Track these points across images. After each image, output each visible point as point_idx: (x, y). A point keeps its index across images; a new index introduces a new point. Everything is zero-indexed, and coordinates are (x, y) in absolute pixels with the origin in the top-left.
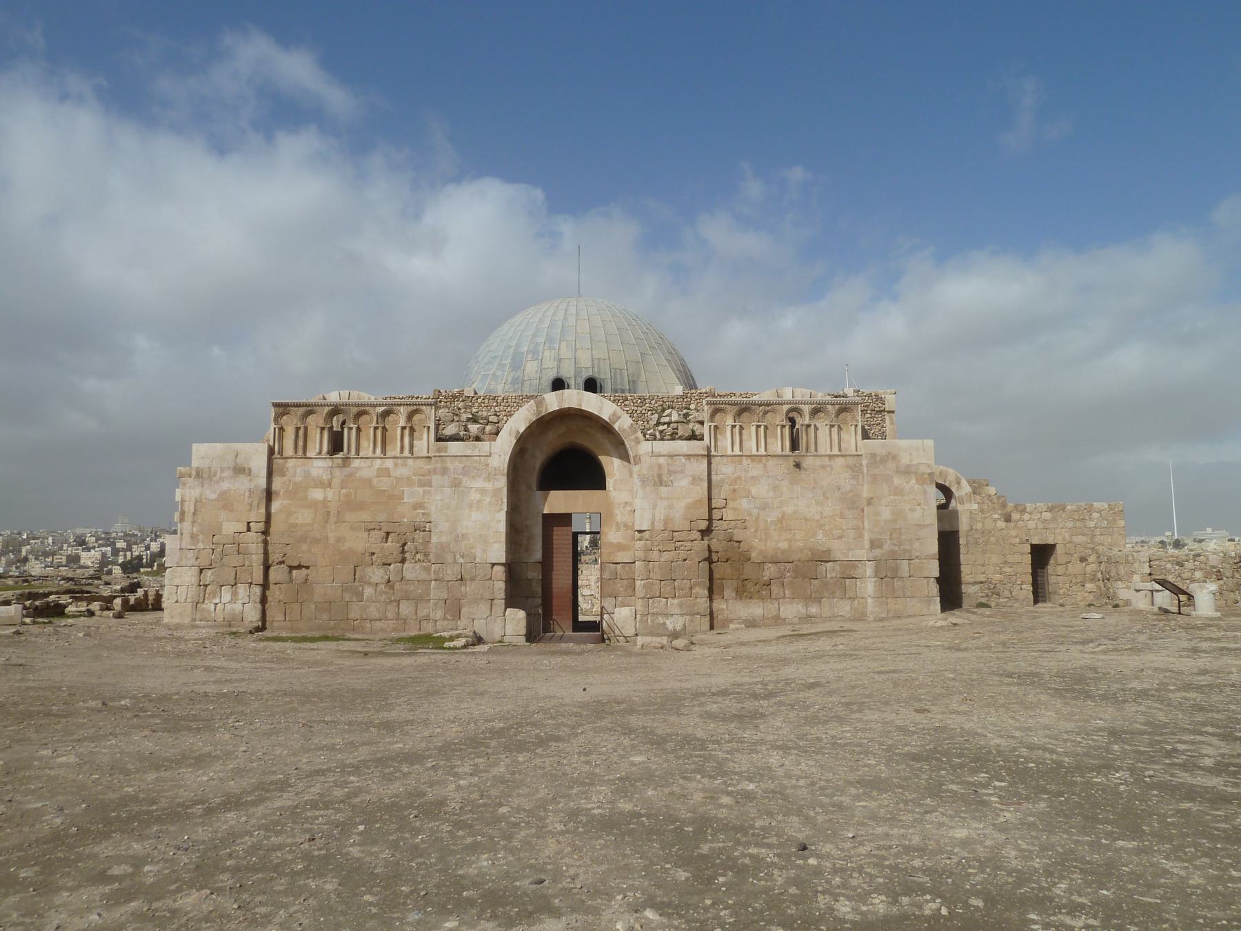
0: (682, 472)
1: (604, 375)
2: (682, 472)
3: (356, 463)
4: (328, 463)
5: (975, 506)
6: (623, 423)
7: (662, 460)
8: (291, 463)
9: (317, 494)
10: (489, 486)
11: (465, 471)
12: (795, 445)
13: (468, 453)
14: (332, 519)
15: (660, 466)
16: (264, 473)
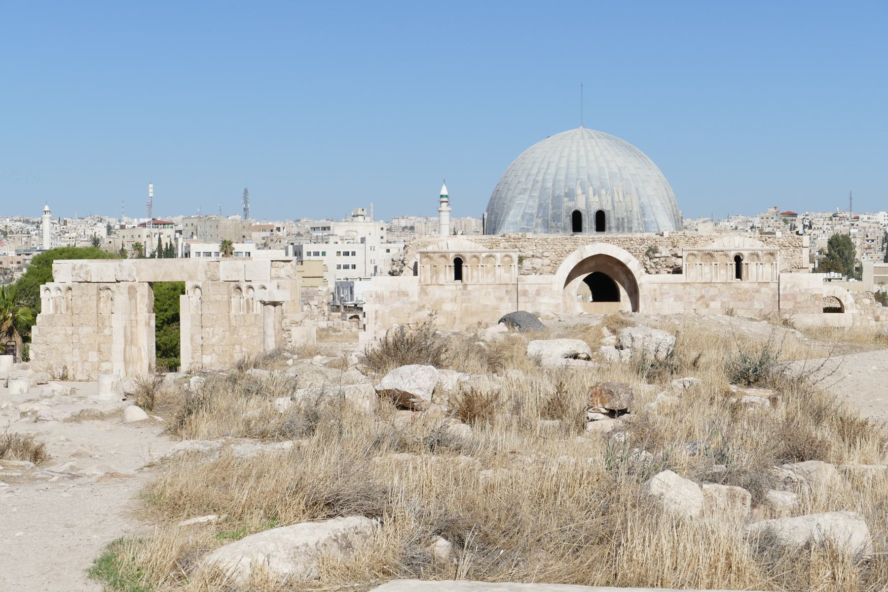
0: (668, 293)
1: (607, 207)
2: (668, 293)
3: (469, 288)
4: (454, 288)
5: (856, 311)
6: (634, 265)
7: (655, 286)
8: (430, 288)
9: (448, 307)
10: (552, 301)
11: (538, 293)
12: (739, 275)
13: (540, 282)
14: (458, 321)
15: (655, 290)
16: (416, 294)
